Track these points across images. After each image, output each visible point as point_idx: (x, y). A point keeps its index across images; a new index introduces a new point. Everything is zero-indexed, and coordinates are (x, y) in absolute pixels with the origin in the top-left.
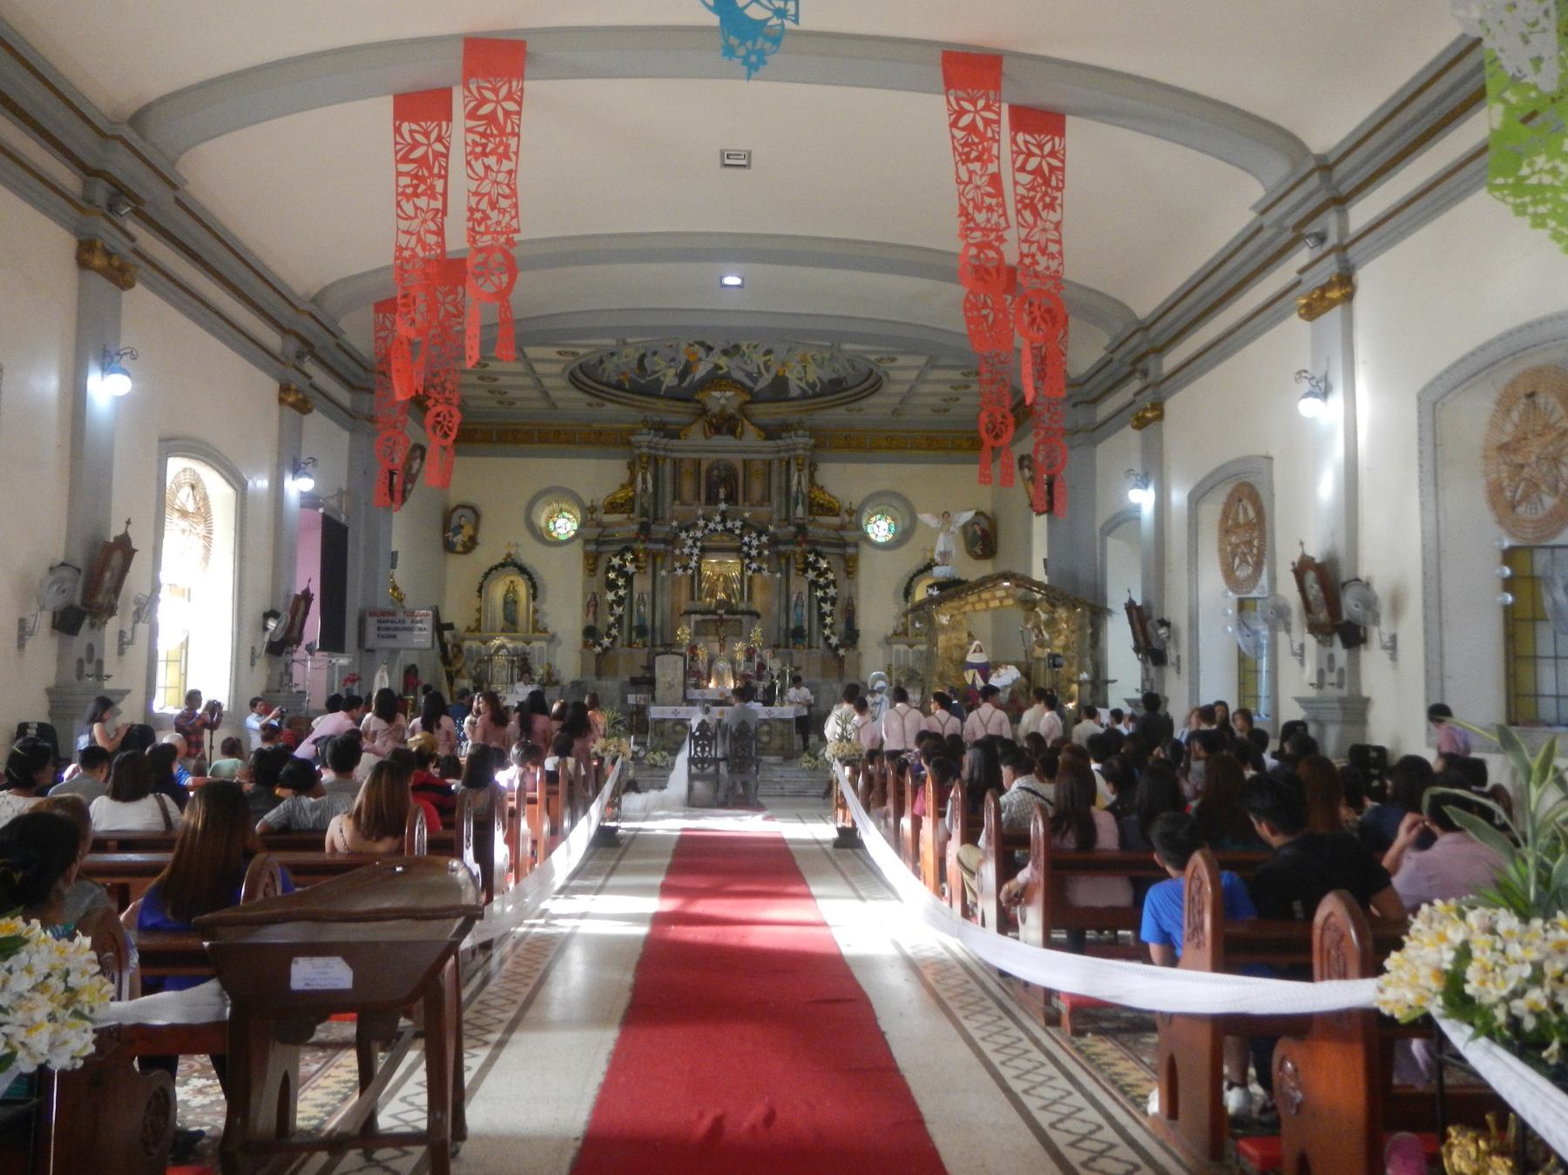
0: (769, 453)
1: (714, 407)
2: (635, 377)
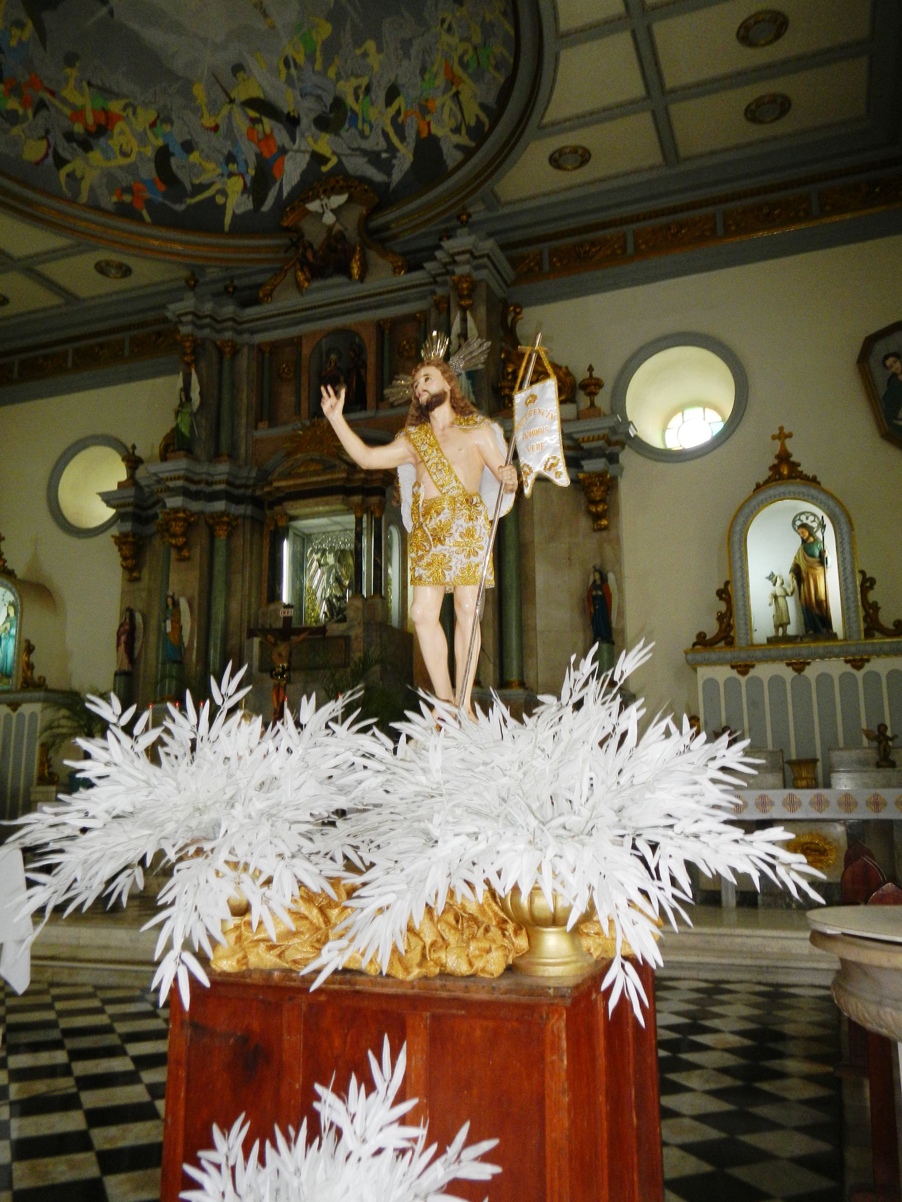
0: (423, 297)
1: (314, 235)
2: (160, 199)
